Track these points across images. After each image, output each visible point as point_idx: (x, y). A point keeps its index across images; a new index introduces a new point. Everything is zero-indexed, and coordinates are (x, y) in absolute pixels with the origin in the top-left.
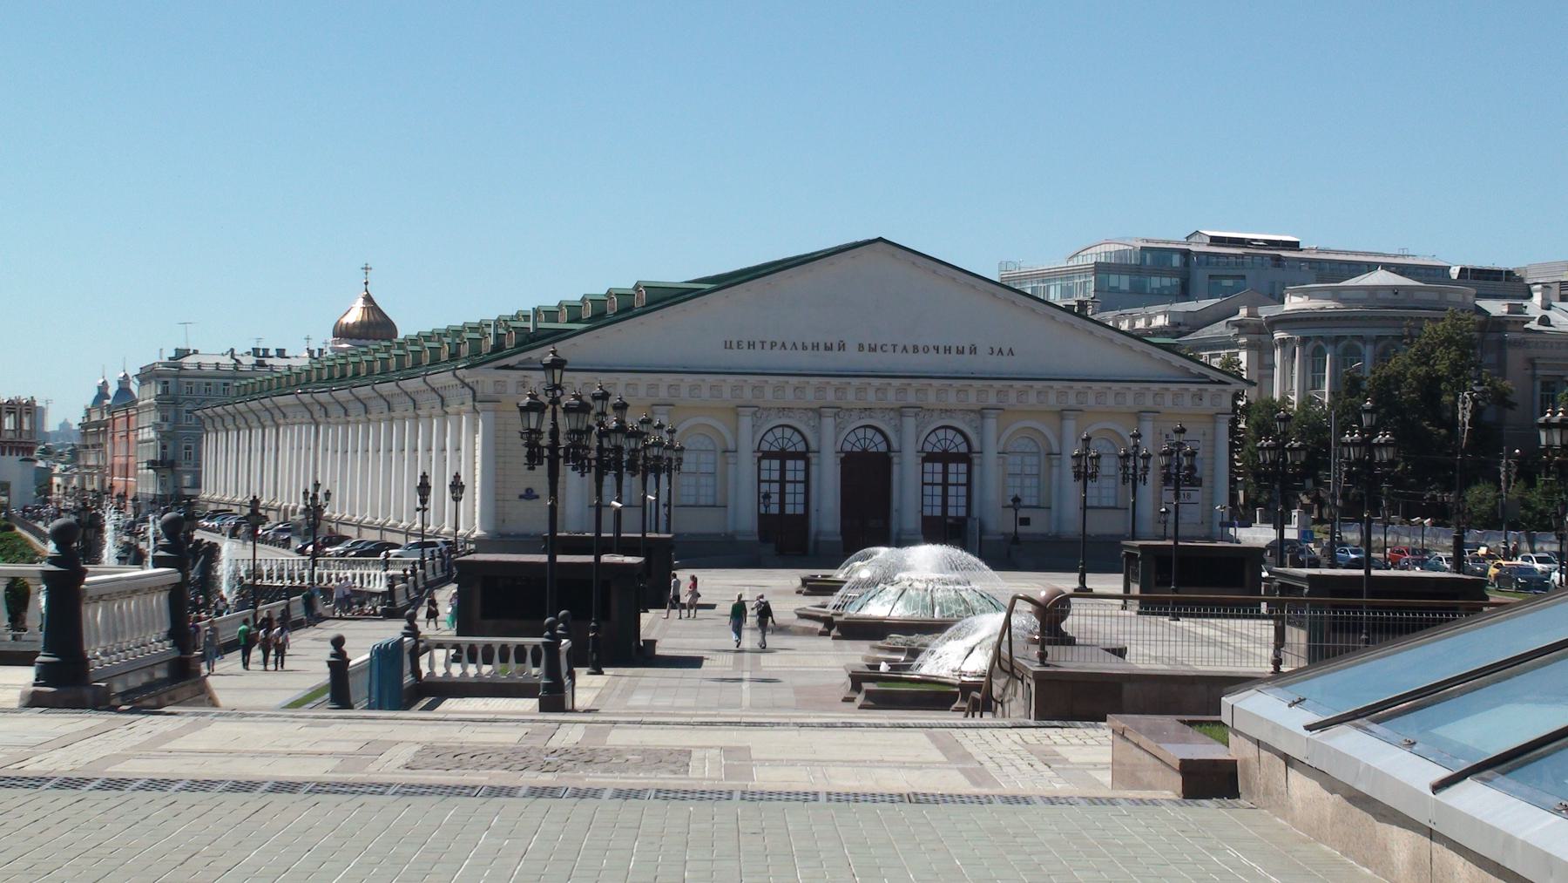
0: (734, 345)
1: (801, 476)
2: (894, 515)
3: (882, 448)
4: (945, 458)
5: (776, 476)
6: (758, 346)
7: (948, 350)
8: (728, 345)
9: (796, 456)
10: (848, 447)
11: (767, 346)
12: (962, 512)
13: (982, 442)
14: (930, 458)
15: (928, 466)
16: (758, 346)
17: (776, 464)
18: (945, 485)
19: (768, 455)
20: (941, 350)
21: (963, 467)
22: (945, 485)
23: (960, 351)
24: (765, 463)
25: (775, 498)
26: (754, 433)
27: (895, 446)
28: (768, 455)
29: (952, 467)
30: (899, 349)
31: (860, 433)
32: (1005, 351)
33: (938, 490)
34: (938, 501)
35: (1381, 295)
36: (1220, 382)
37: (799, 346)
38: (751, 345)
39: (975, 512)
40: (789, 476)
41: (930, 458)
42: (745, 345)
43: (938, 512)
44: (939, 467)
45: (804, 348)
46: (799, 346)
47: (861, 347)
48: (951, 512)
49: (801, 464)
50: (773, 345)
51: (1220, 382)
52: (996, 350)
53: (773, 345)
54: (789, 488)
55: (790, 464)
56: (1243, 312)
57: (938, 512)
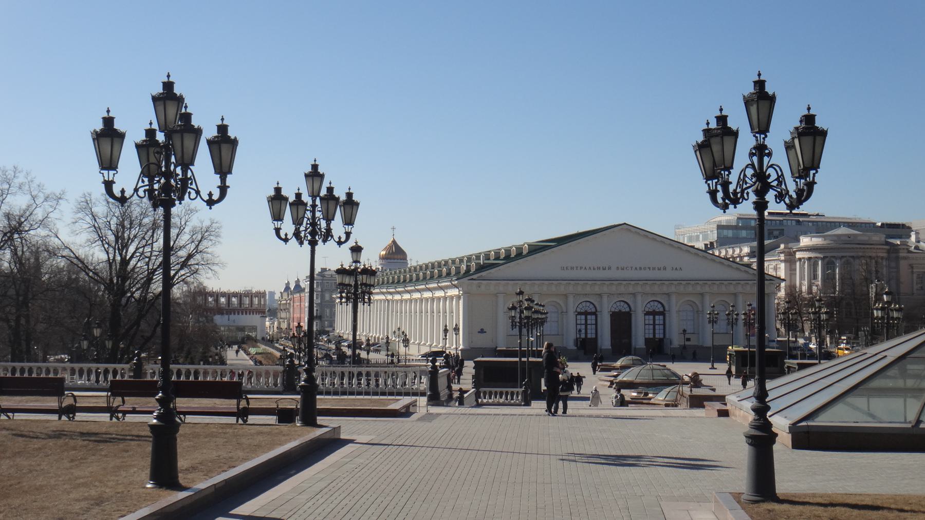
1: (594, 322)
2: (633, 338)
3: (627, 310)
4: (654, 313)
5: (583, 322)
7: (654, 269)
8: (563, 268)
9: (591, 314)
10: (613, 310)
12: (662, 336)
13: (669, 306)
14: (647, 313)
15: (647, 317)
17: (583, 317)
18: (654, 325)
19: (580, 314)
21: (661, 317)
22: (654, 325)
23: (659, 269)
24: (579, 317)
25: (583, 331)
27: (633, 309)
28: (580, 314)
29: (657, 317)
31: (618, 304)
33: (651, 327)
34: (651, 331)
35: (842, 238)
38: (572, 268)
39: (667, 336)
40: (589, 322)
41: (647, 313)
43: (651, 336)
44: (651, 317)
48: (657, 336)
49: (593, 317)
50: (581, 268)
54: (589, 327)
55: (589, 317)
56: (782, 246)
57: (651, 336)
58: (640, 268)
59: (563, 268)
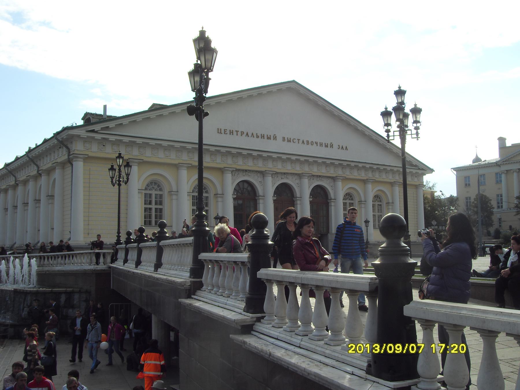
0: (223, 132)
6: (235, 133)
7: (321, 145)
8: (219, 131)
11: (239, 133)
13: (335, 193)
16: (235, 133)
20: (319, 144)
23: (326, 146)
26: (273, 186)
30: (301, 142)
32: (344, 148)
36: (423, 169)
37: (255, 136)
38: (231, 132)
42: (228, 132)
45: (258, 137)
46: (255, 136)
47: (284, 139)
51: (423, 169)
52: (341, 147)
53: (242, 133)
58: (308, 142)
59: (219, 131)
